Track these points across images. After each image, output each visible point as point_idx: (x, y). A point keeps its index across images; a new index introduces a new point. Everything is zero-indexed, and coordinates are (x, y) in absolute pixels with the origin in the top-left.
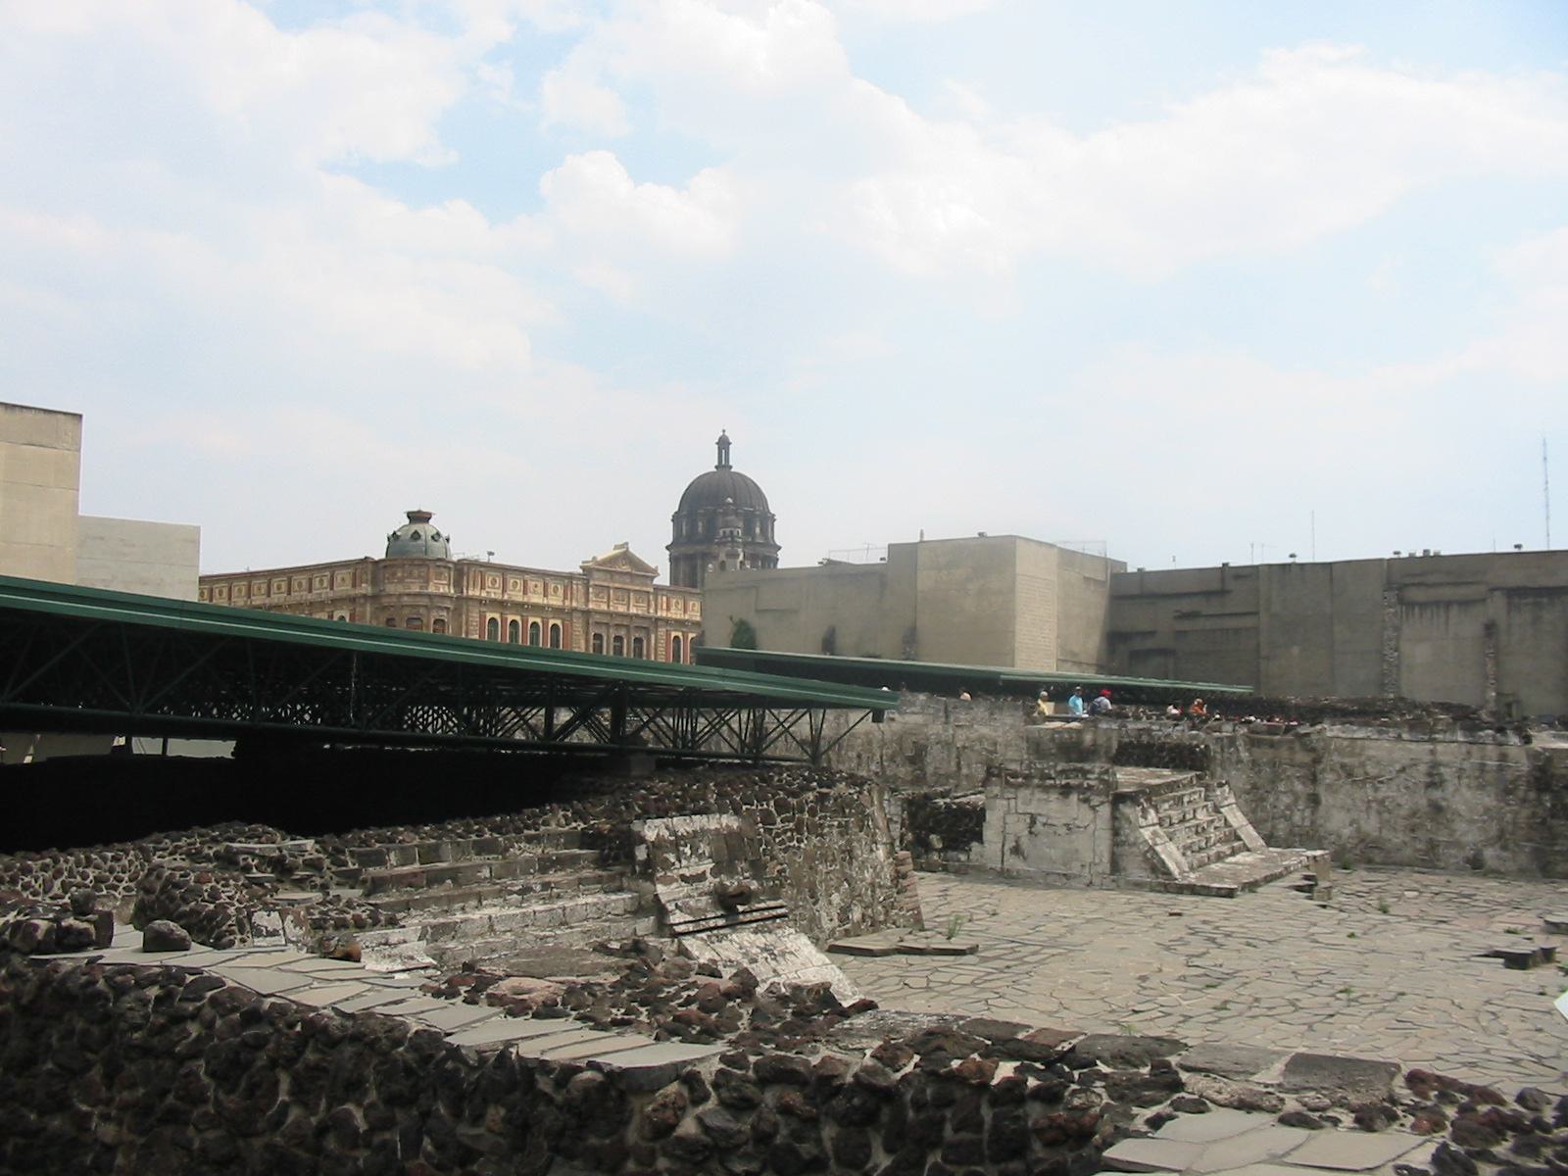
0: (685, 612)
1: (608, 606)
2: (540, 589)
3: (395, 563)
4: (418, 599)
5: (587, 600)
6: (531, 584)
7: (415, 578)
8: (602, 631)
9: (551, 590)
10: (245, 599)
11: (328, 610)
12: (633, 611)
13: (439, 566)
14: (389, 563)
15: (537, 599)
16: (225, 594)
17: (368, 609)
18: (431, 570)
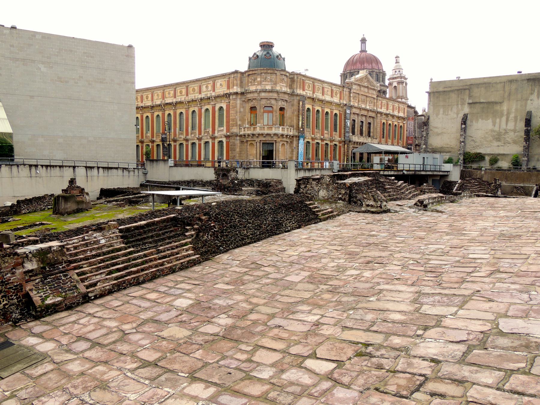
0: (387, 110)
1: (358, 104)
2: (329, 93)
3: (256, 72)
4: (271, 94)
5: (350, 101)
6: (326, 90)
7: (268, 82)
8: (355, 117)
9: (334, 94)
10: (161, 100)
11: (212, 103)
12: (368, 107)
13: (282, 74)
14: (251, 73)
15: (328, 98)
16: (150, 98)
17: (238, 102)
18: (278, 77)
